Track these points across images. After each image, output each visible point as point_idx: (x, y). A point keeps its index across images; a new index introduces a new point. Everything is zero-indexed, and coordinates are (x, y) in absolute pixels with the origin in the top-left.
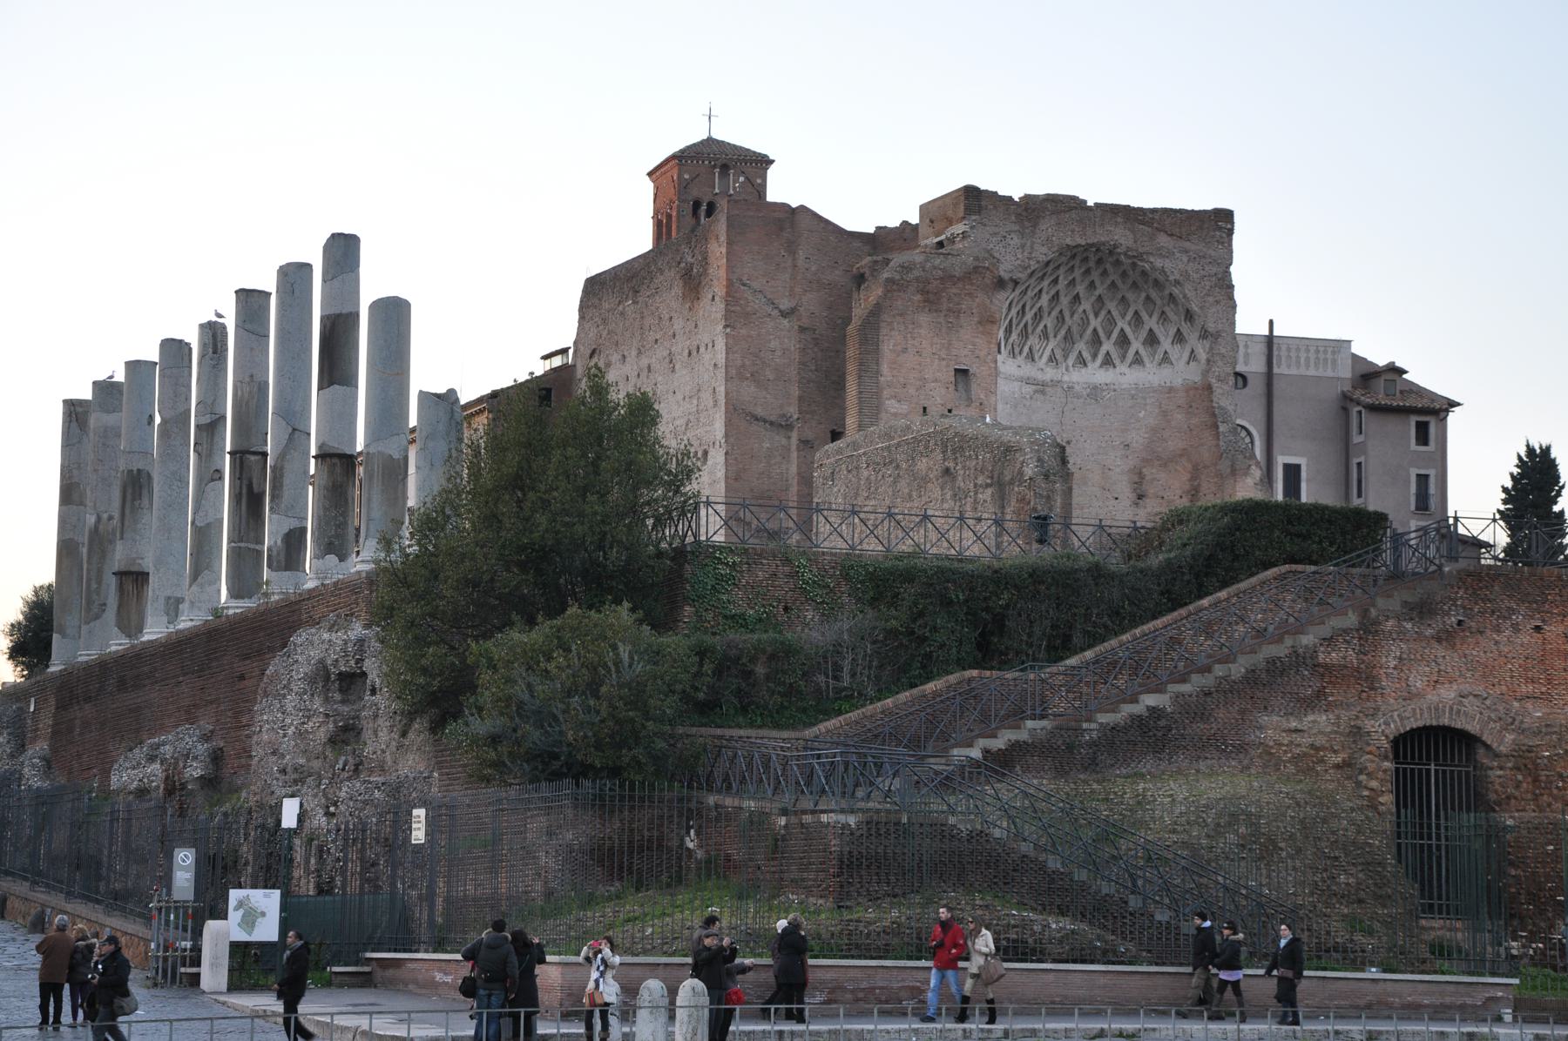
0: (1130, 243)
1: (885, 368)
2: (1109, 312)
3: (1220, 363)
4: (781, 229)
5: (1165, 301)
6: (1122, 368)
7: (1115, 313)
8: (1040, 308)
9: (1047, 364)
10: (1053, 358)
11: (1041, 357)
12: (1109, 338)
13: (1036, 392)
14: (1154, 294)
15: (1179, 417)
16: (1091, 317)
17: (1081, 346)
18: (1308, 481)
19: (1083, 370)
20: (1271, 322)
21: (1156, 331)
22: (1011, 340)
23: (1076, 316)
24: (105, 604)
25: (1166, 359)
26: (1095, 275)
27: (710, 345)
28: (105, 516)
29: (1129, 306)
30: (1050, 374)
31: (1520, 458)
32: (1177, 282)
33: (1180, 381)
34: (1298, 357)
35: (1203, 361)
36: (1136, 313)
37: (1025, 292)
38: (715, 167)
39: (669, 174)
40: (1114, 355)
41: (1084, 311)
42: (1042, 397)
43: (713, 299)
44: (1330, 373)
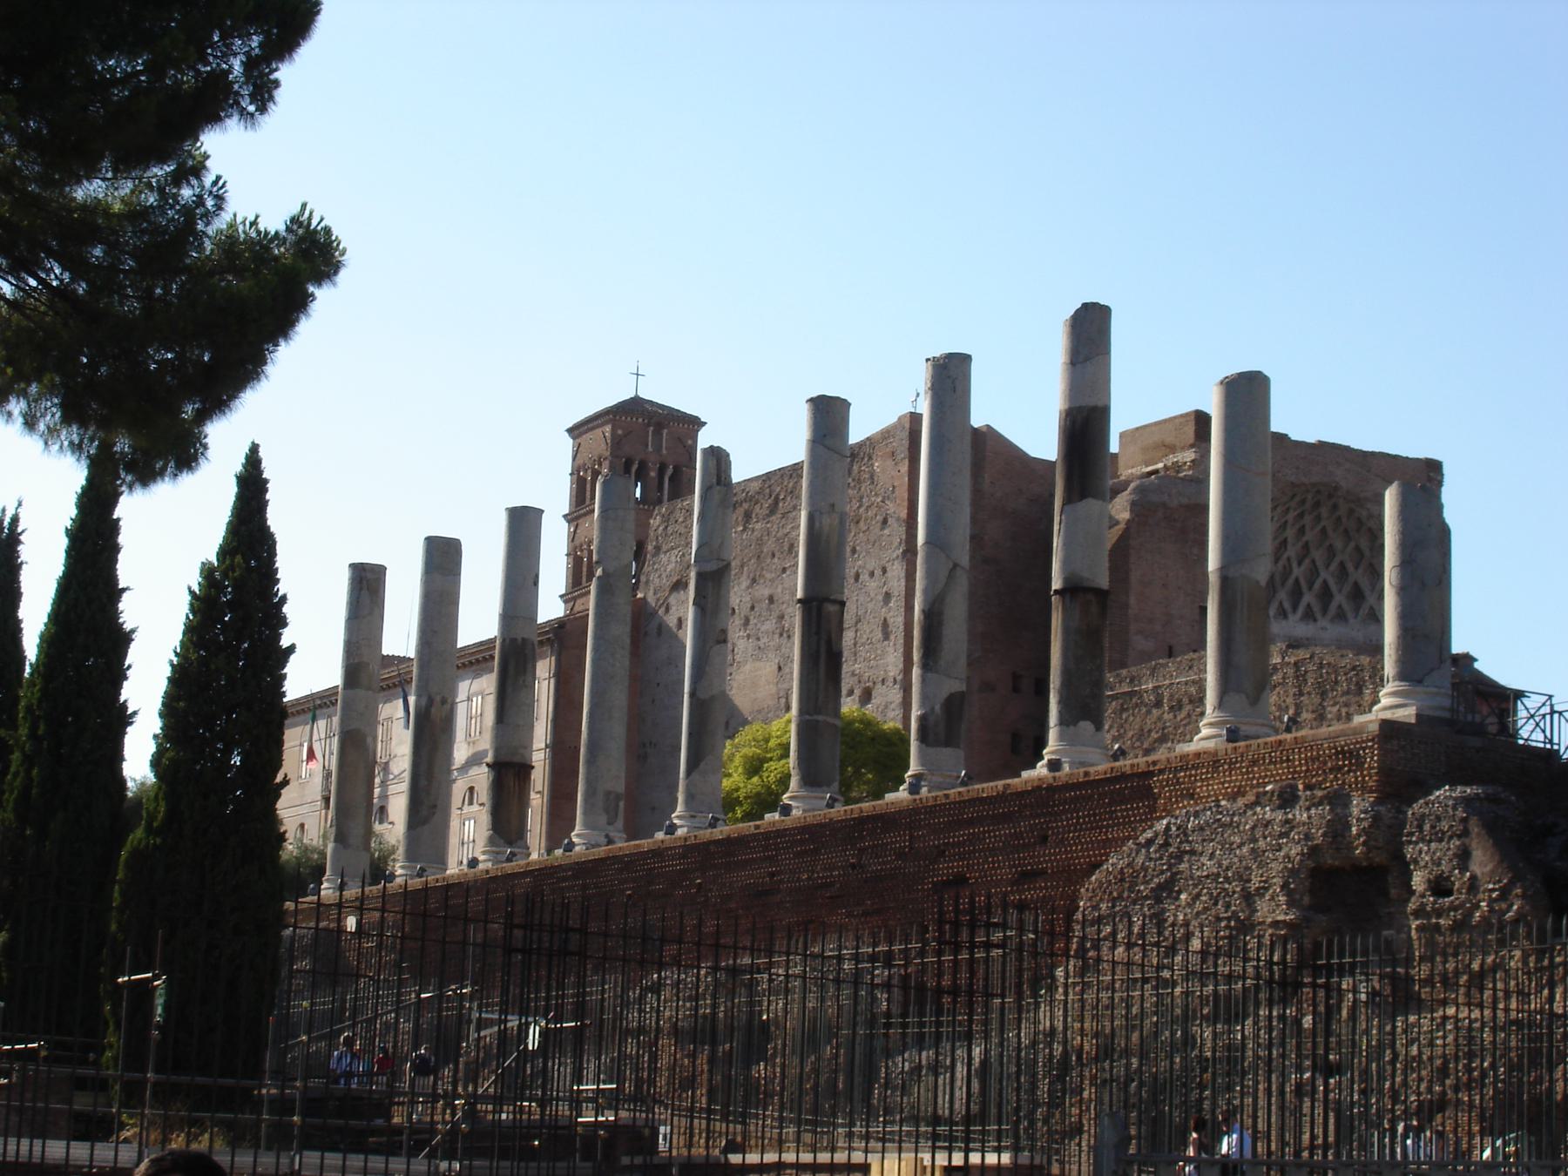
1: (1132, 601)
2: (1313, 562)
6: (1322, 622)
7: (1319, 563)
12: (1310, 589)
16: (1295, 565)
19: (1284, 622)
24: (435, 806)
26: (1308, 520)
27: (878, 572)
28: (438, 699)
29: (1334, 556)
38: (649, 425)
39: (598, 431)
43: (885, 521)
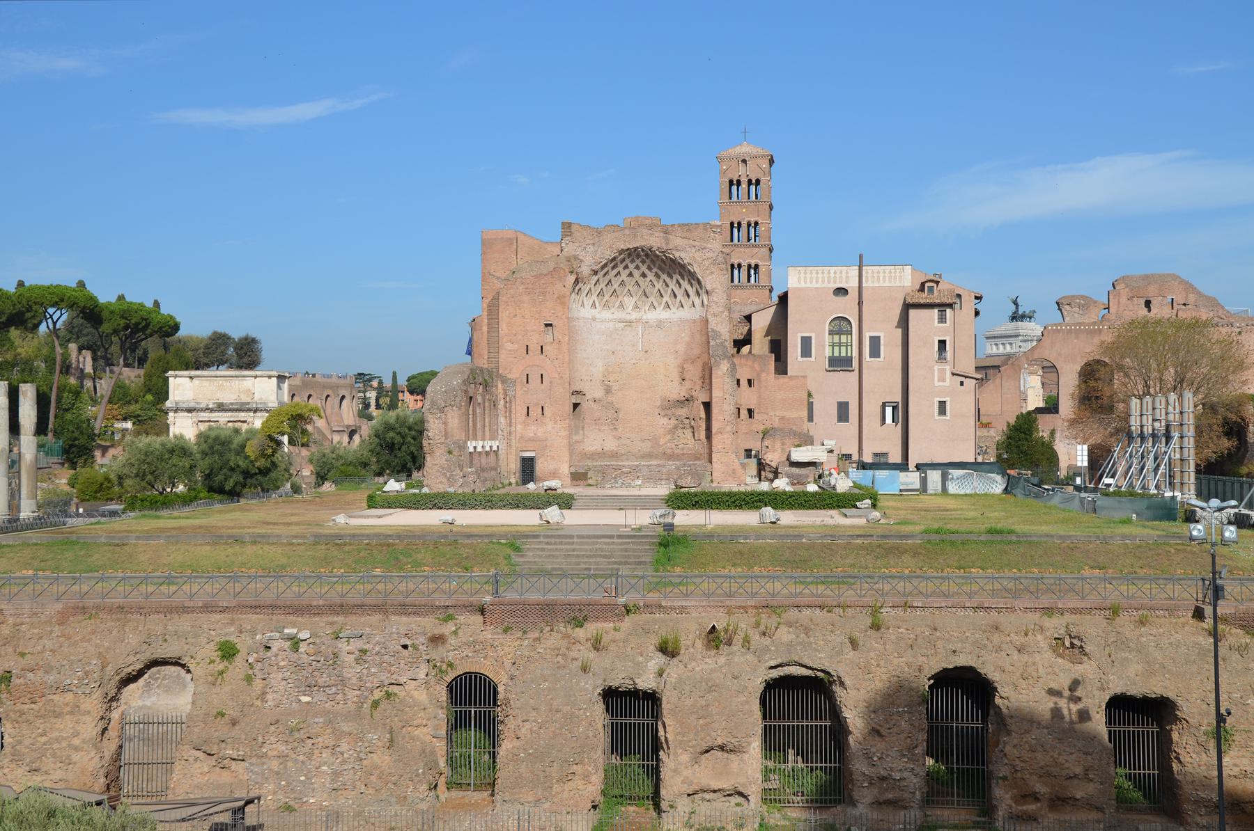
0: (659, 245)
3: (714, 307)
4: (512, 244)
6: (674, 309)
10: (636, 307)
15: (698, 336)
18: (884, 345)
20: (861, 256)
30: (634, 316)
32: (690, 264)
33: (698, 317)
34: (878, 277)
42: (630, 329)
44: (898, 284)
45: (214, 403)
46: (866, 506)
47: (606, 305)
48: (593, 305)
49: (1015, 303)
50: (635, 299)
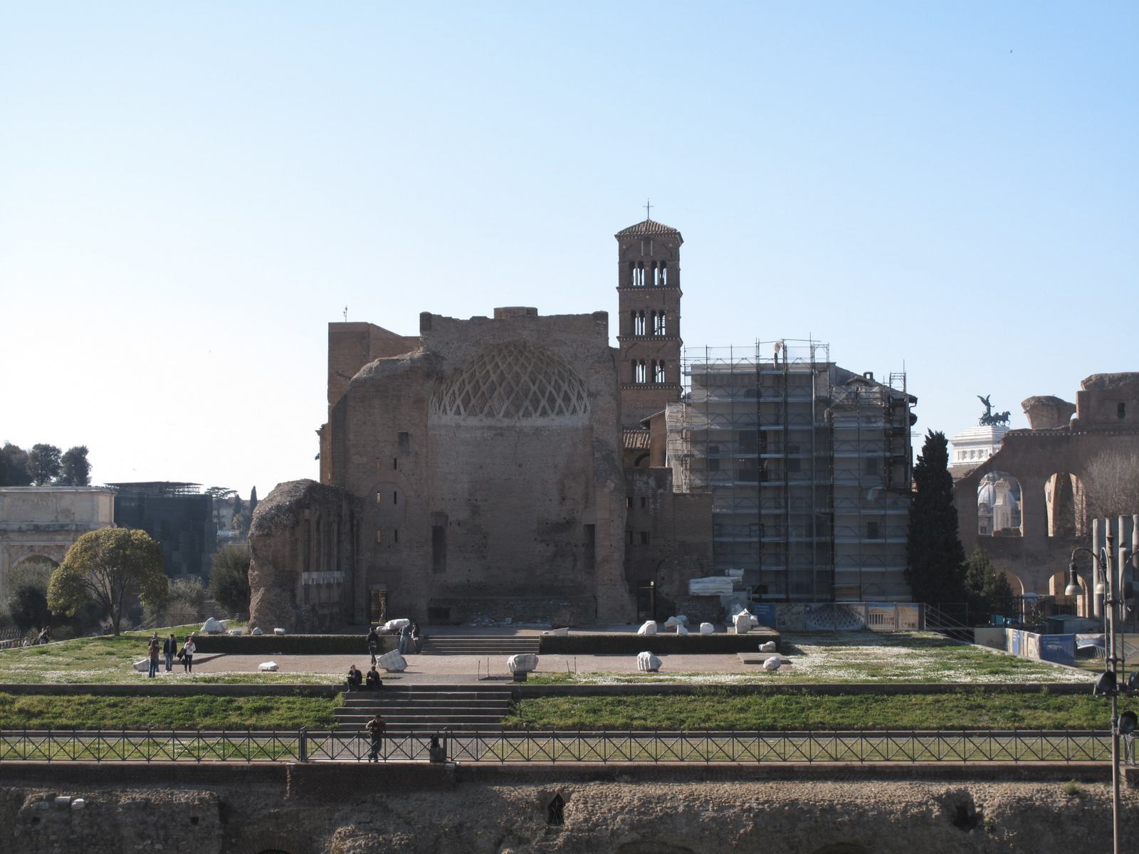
2: (541, 381)
5: (568, 373)
6: (553, 416)
8: (493, 382)
9: (504, 416)
10: (507, 415)
11: (499, 413)
12: (544, 396)
13: (496, 434)
14: (562, 370)
17: (527, 403)
19: (529, 419)
21: (569, 392)
22: (471, 405)
23: (520, 385)
25: (574, 411)
26: (522, 360)
30: (506, 422)
31: (927, 437)
35: (589, 412)
36: (556, 381)
37: (473, 375)
40: (548, 408)
41: (525, 381)
45: (28, 525)
46: (770, 649)
47: (473, 413)
48: (458, 413)
49: (986, 402)
50: (507, 403)
